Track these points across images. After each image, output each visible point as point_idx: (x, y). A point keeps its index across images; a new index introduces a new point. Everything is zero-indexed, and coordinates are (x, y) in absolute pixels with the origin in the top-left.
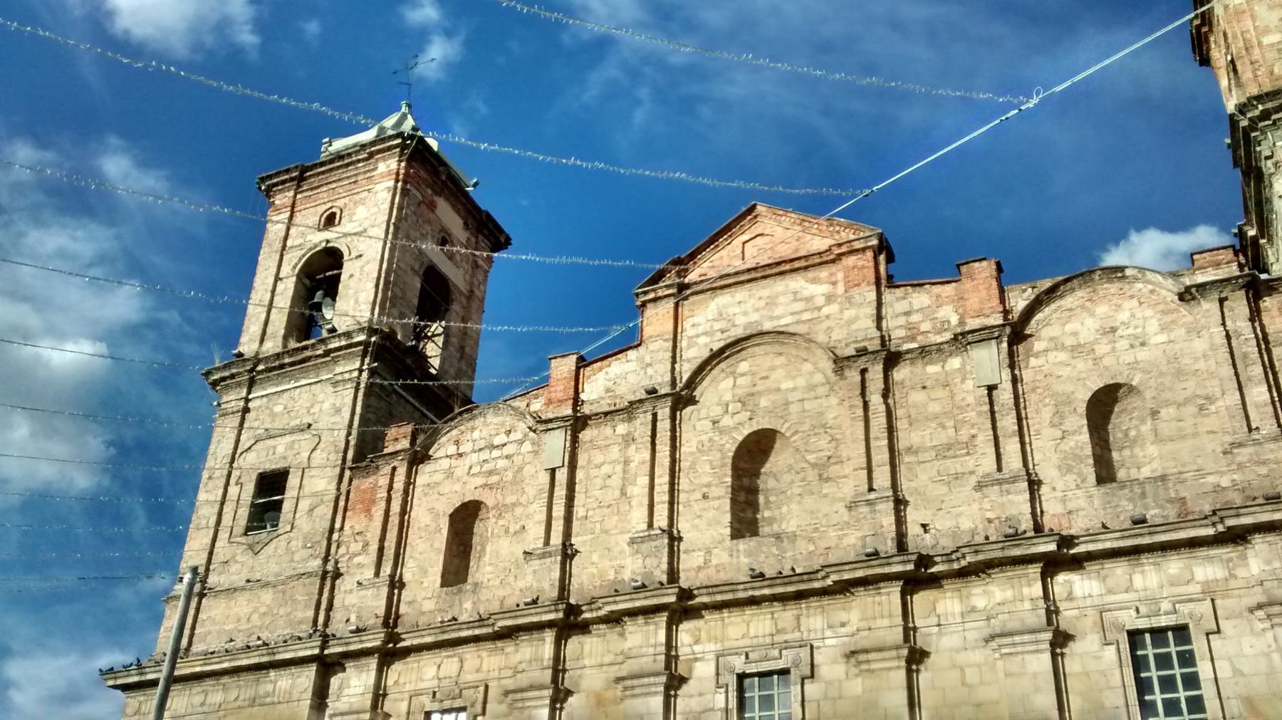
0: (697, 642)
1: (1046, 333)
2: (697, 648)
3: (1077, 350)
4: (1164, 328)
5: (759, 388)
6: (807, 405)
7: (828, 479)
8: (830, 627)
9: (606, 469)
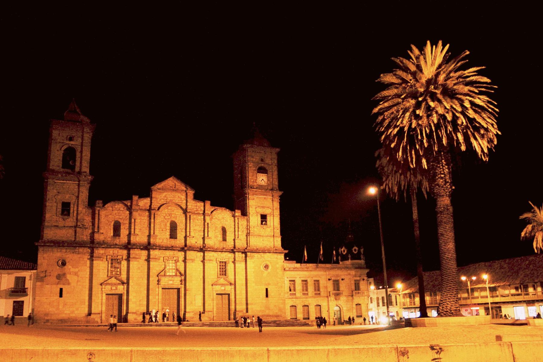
1: (216, 216)
2: (161, 255)
3: (219, 220)
5: (172, 213)
9: (144, 221)
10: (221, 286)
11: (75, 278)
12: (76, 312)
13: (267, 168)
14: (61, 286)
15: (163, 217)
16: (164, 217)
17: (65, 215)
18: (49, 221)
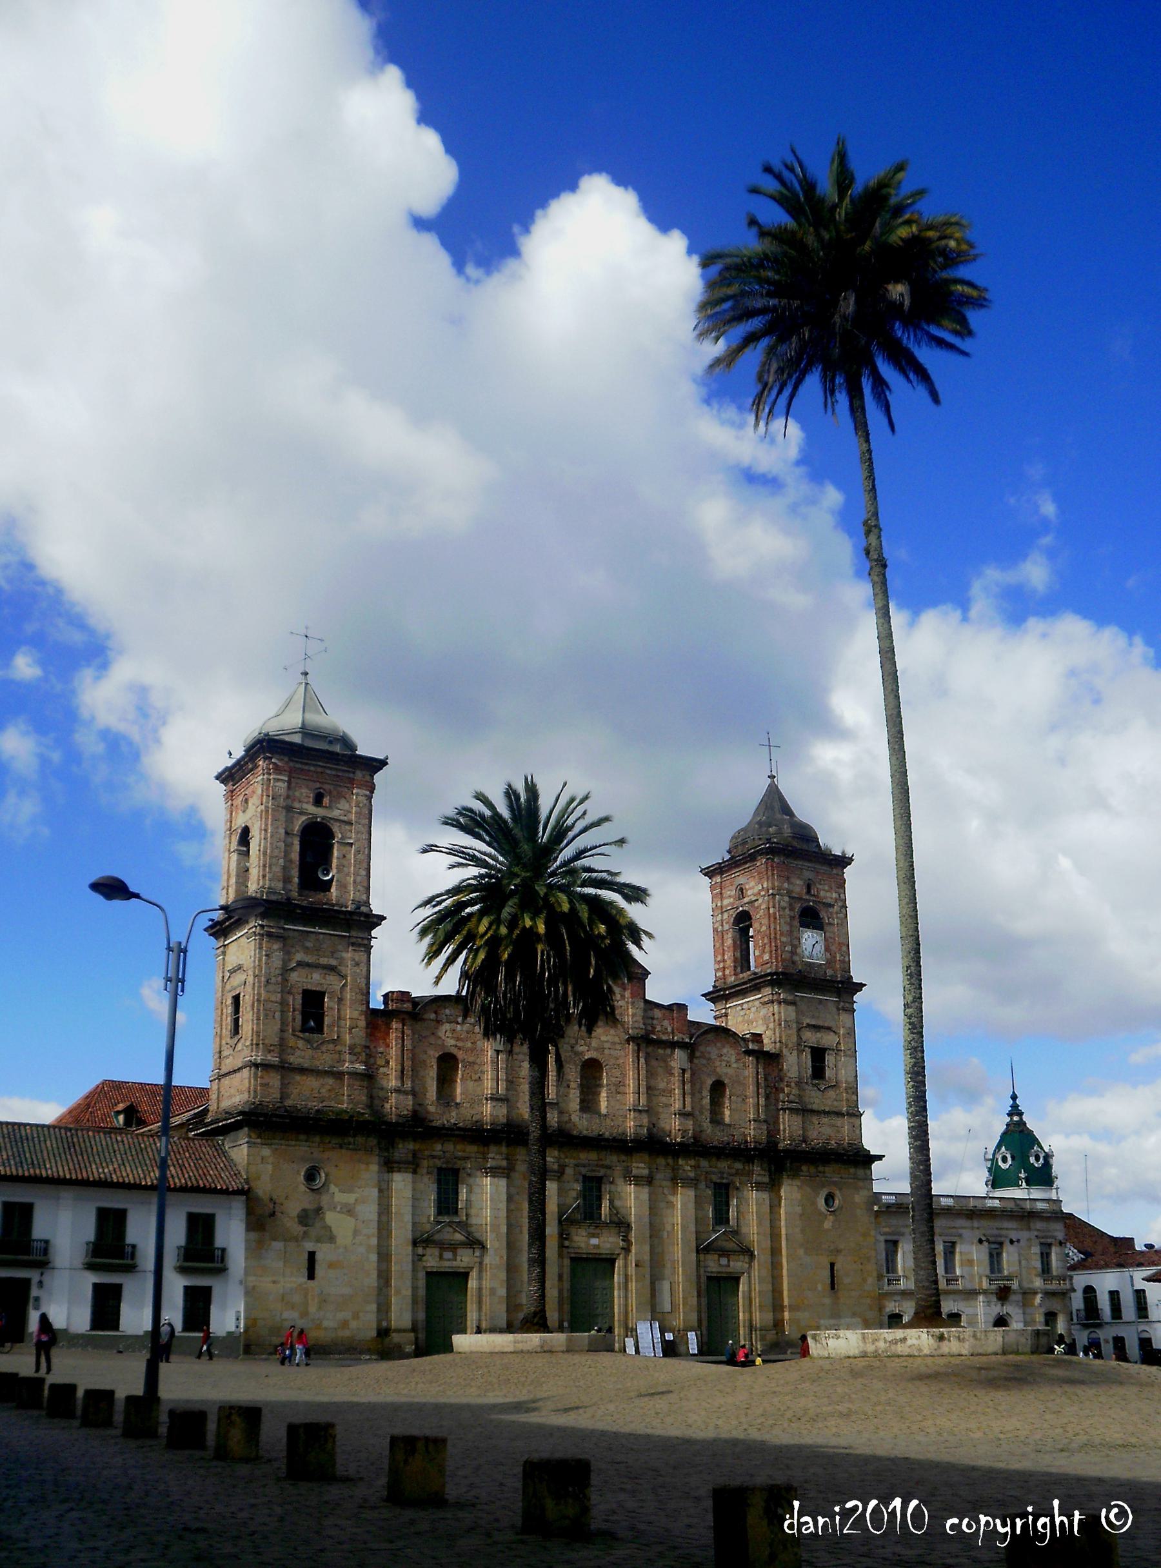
0: (566, 1157)
2: (566, 1160)
4: (737, 1061)
6: (612, 1052)
7: (619, 1093)
8: (619, 1161)
10: (720, 1256)
11: (349, 1222)
12: (354, 1324)
13: (823, 914)
14: (309, 1246)
15: (570, 1049)
16: (573, 1047)
17: (311, 1030)
18: (272, 1048)
